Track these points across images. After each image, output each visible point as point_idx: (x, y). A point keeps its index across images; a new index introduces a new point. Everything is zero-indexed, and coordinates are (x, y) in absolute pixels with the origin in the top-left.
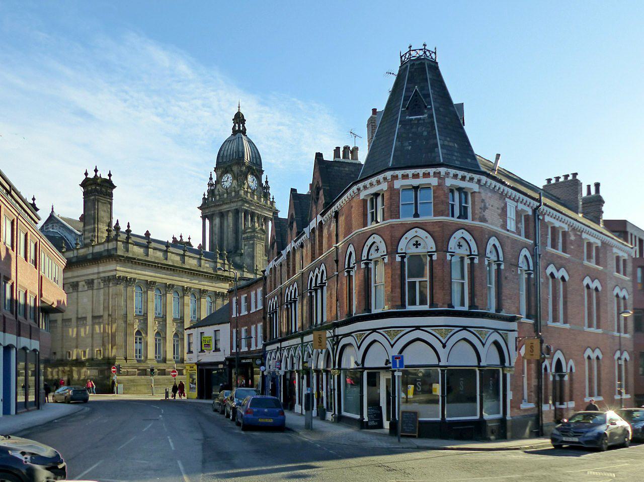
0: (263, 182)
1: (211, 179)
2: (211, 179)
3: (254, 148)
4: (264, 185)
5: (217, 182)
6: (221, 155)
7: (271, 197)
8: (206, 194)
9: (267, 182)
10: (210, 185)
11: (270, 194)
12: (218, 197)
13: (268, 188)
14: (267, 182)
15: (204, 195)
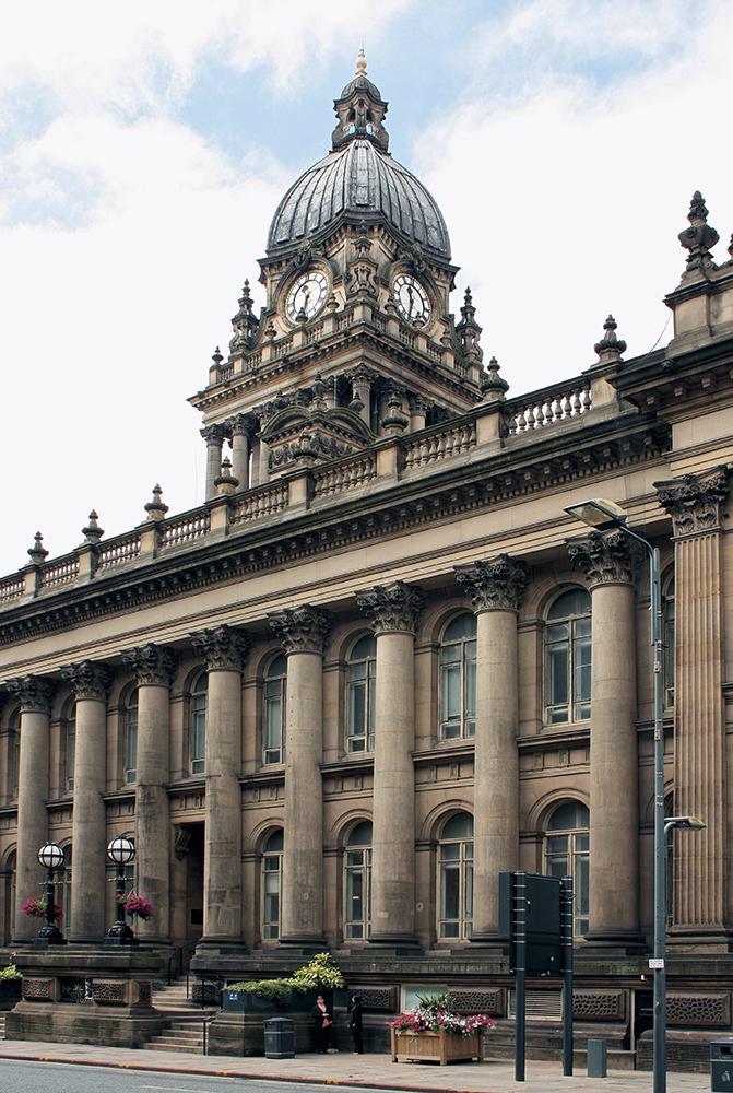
0: (455, 303)
1: (247, 302)
2: (247, 302)
3: (421, 196)
4: (458, 319)
5: (269, 313)
6: (288, 213)
7: (486, 362)
8: (226, 353)
9: (468, 310)
10: (245, 320)
11: (479, 355)
12: (266, 354)
13: (469, 328)
14: (468, 310)
15: (218, 358)
